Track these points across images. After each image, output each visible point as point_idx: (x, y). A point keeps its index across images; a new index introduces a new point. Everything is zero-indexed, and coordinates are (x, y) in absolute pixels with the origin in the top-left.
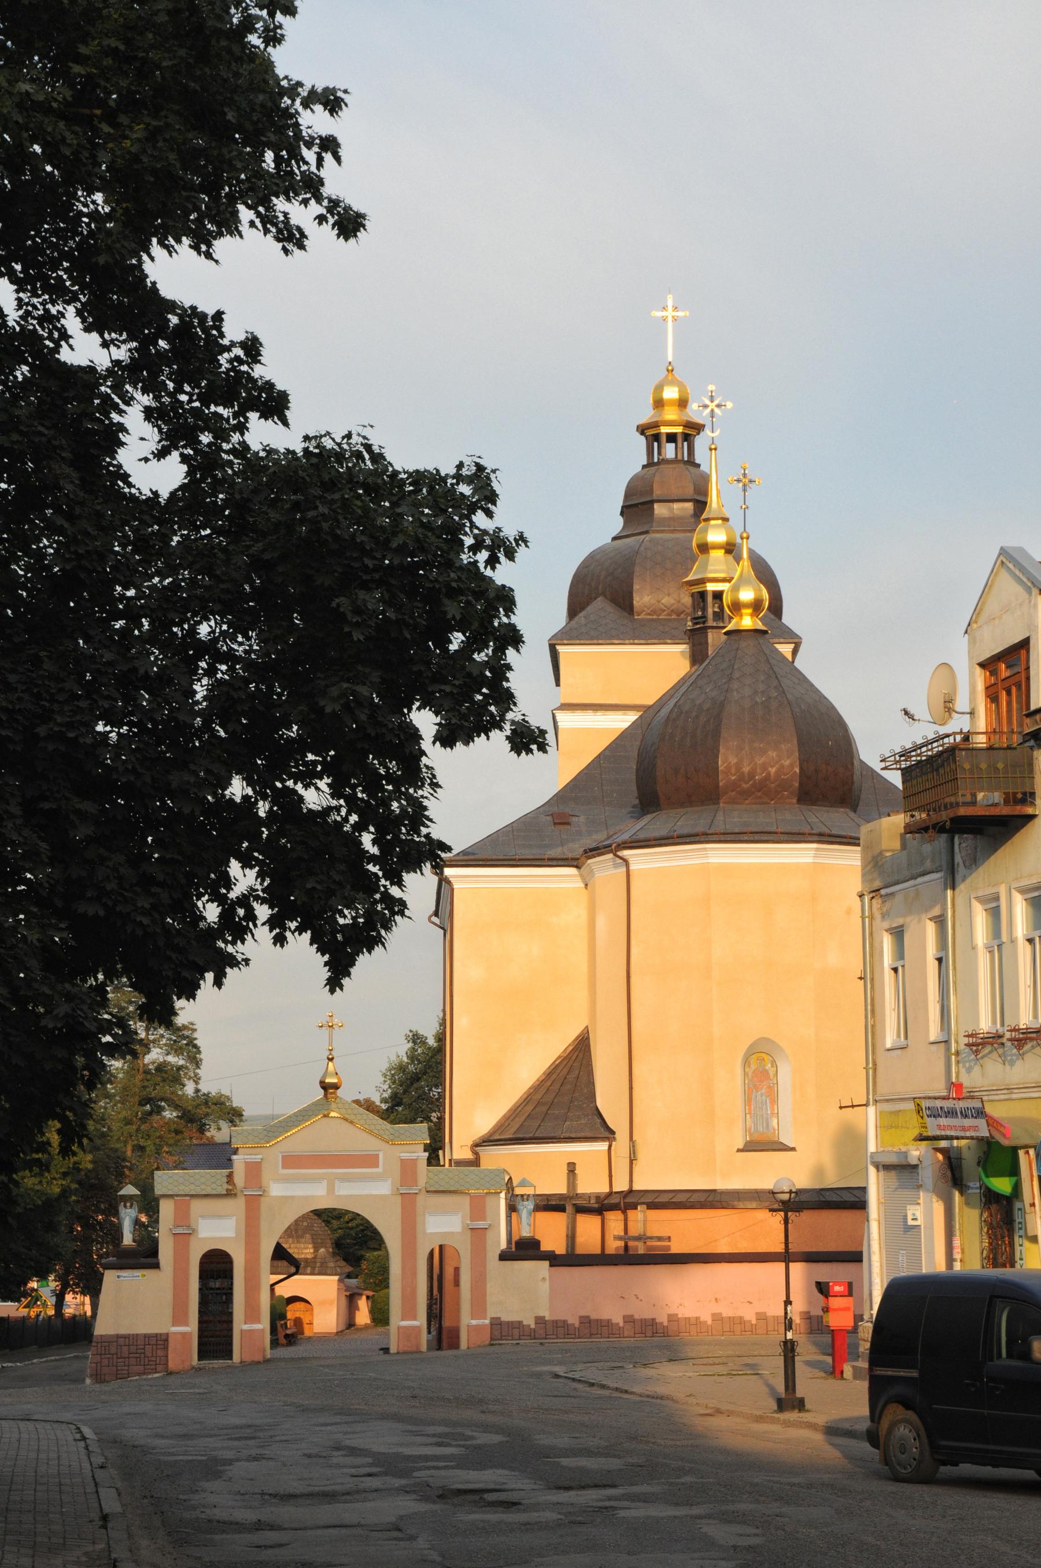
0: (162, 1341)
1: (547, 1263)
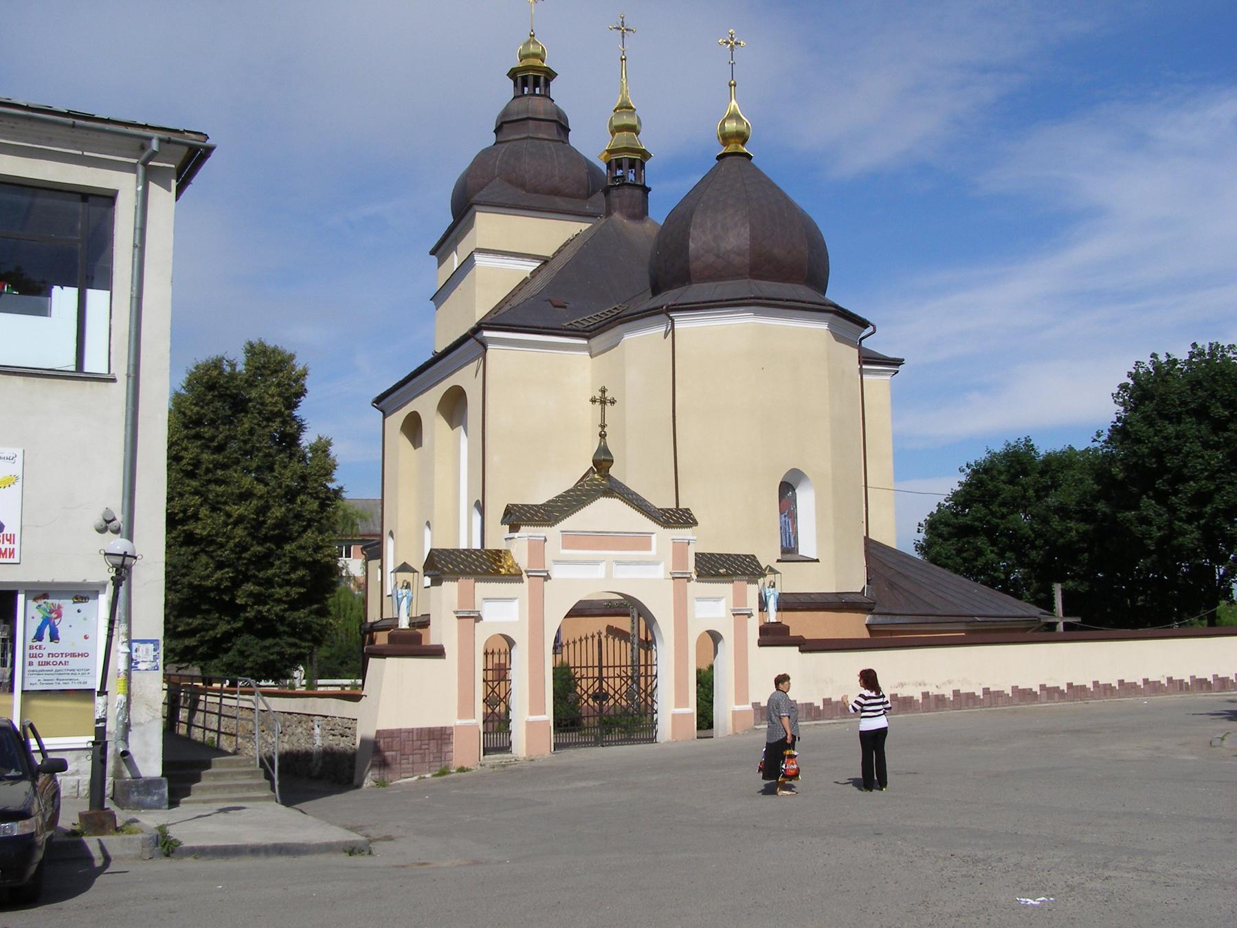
0: (439, 737)
1: (797, 648)
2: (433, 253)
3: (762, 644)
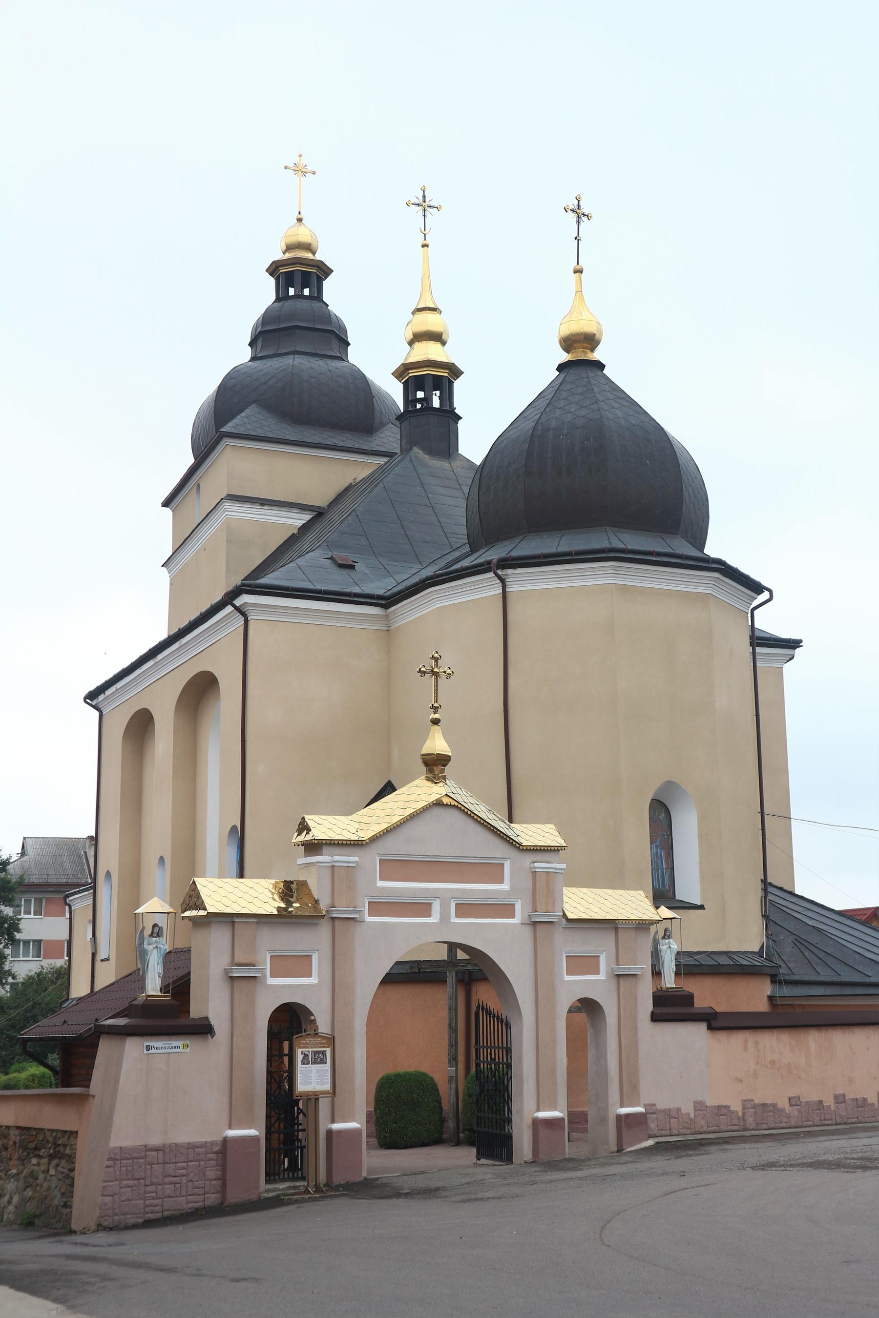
2: (166, 504)
3: (655, 1018)
